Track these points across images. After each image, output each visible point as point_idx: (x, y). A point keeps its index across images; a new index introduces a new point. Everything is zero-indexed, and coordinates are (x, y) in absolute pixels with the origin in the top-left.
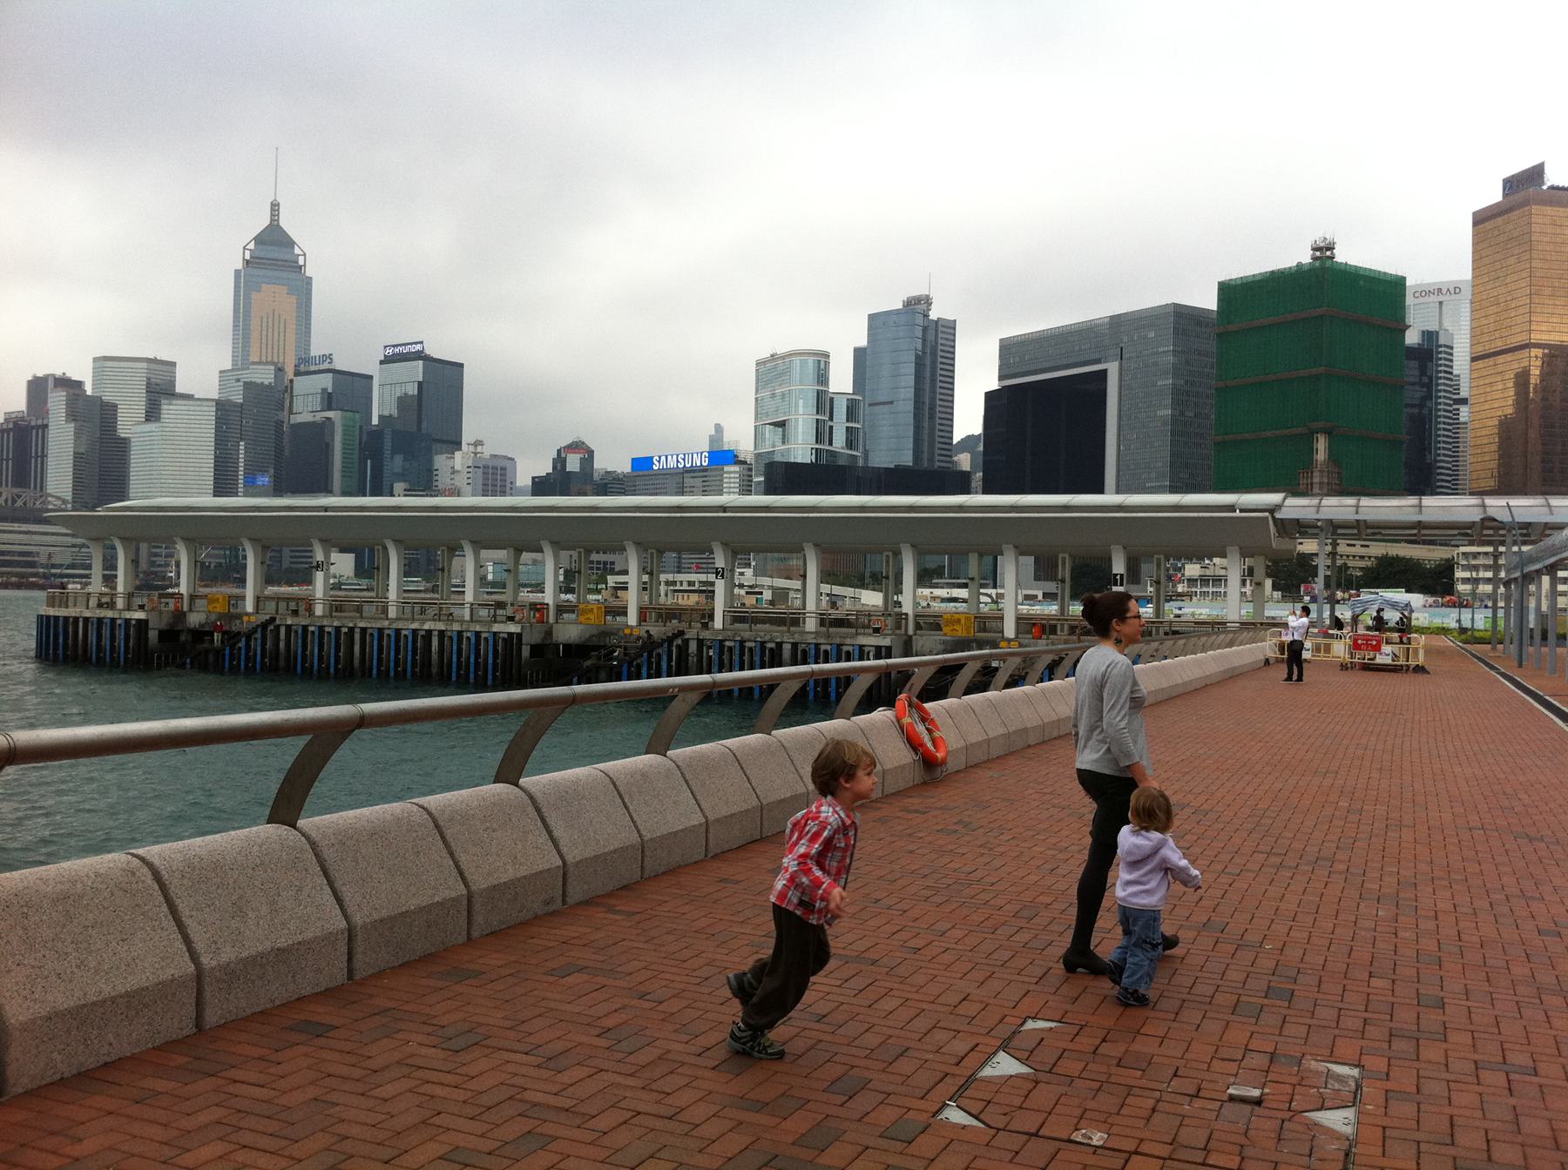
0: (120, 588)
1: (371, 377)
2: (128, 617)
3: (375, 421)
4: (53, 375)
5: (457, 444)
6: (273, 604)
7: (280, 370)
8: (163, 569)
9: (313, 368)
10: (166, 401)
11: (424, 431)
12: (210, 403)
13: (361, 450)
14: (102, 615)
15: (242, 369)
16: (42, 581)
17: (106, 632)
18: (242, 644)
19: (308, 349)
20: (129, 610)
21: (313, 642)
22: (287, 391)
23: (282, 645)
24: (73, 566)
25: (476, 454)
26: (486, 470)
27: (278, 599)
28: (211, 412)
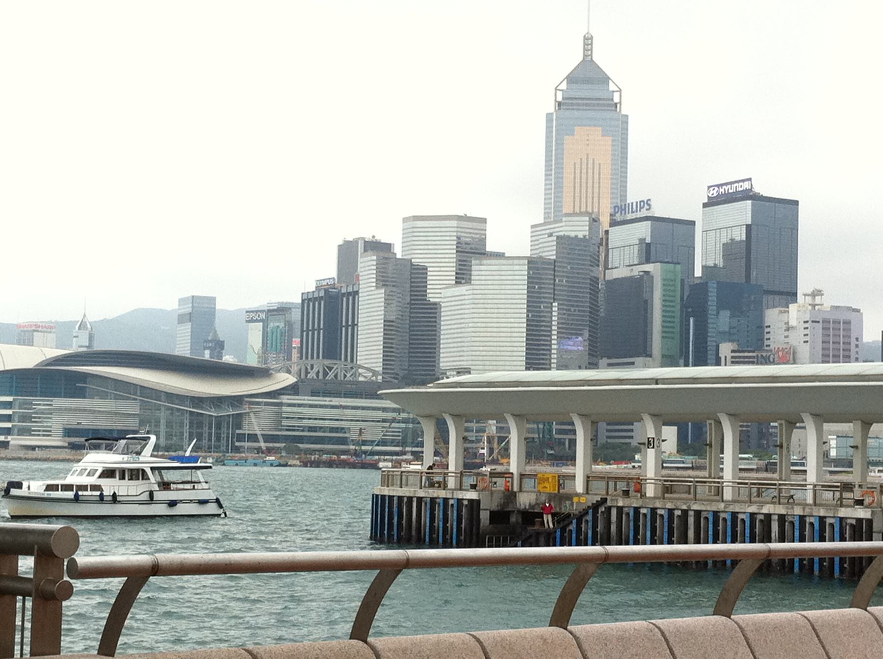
0: (452, 468)
1: (693, 223)
2: (460, 497)
3: (698, 273)
4: (363, 238)
5: (792, 296)
6: (603, 484)
7: (595, 221)
8: (474, 445)
9: (629, 217)
10: (477, 262)
11: (753, 282)
12: (522, 262)
13: (683, 307)
14: (435, 495)
15: (555, 222)
16: (353, 459)
17: (439, 513)
18: (573, 527)
19: (624, 196)
20: (461, 489)
21: (645, 526)
22: (601, 244)
23: (613, 528)
24: (383, 443)
25: (814, 306)
26: (826, 325)
27: (607, 478)
28: (522, 272)
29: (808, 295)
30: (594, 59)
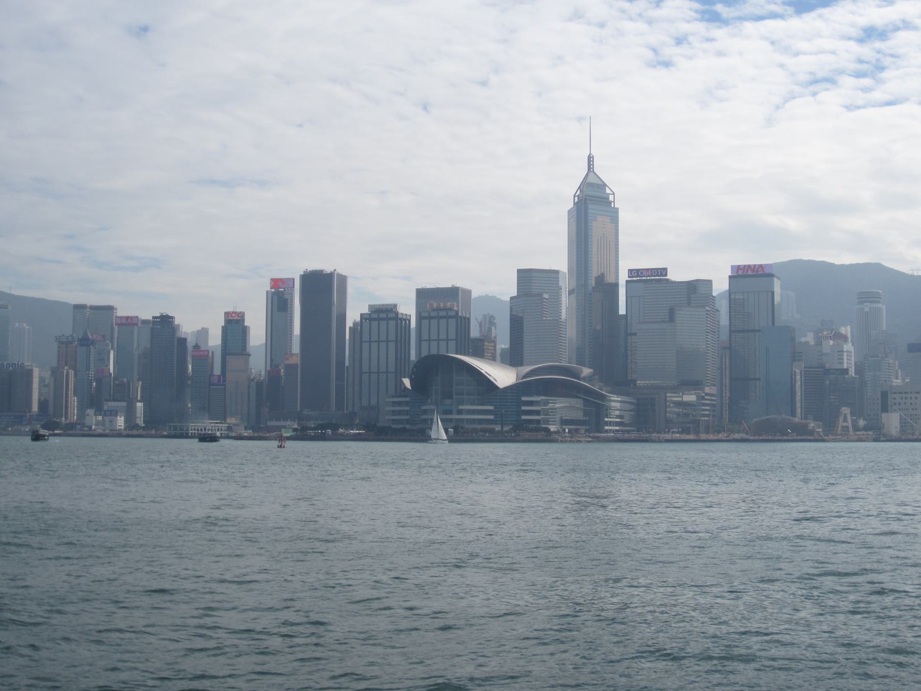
30: (595, 170)
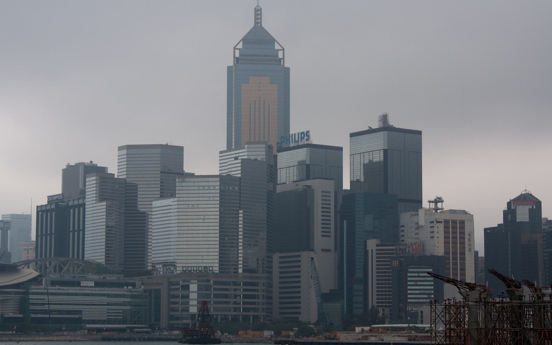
3: (346, 185)
29: (432, 202)
